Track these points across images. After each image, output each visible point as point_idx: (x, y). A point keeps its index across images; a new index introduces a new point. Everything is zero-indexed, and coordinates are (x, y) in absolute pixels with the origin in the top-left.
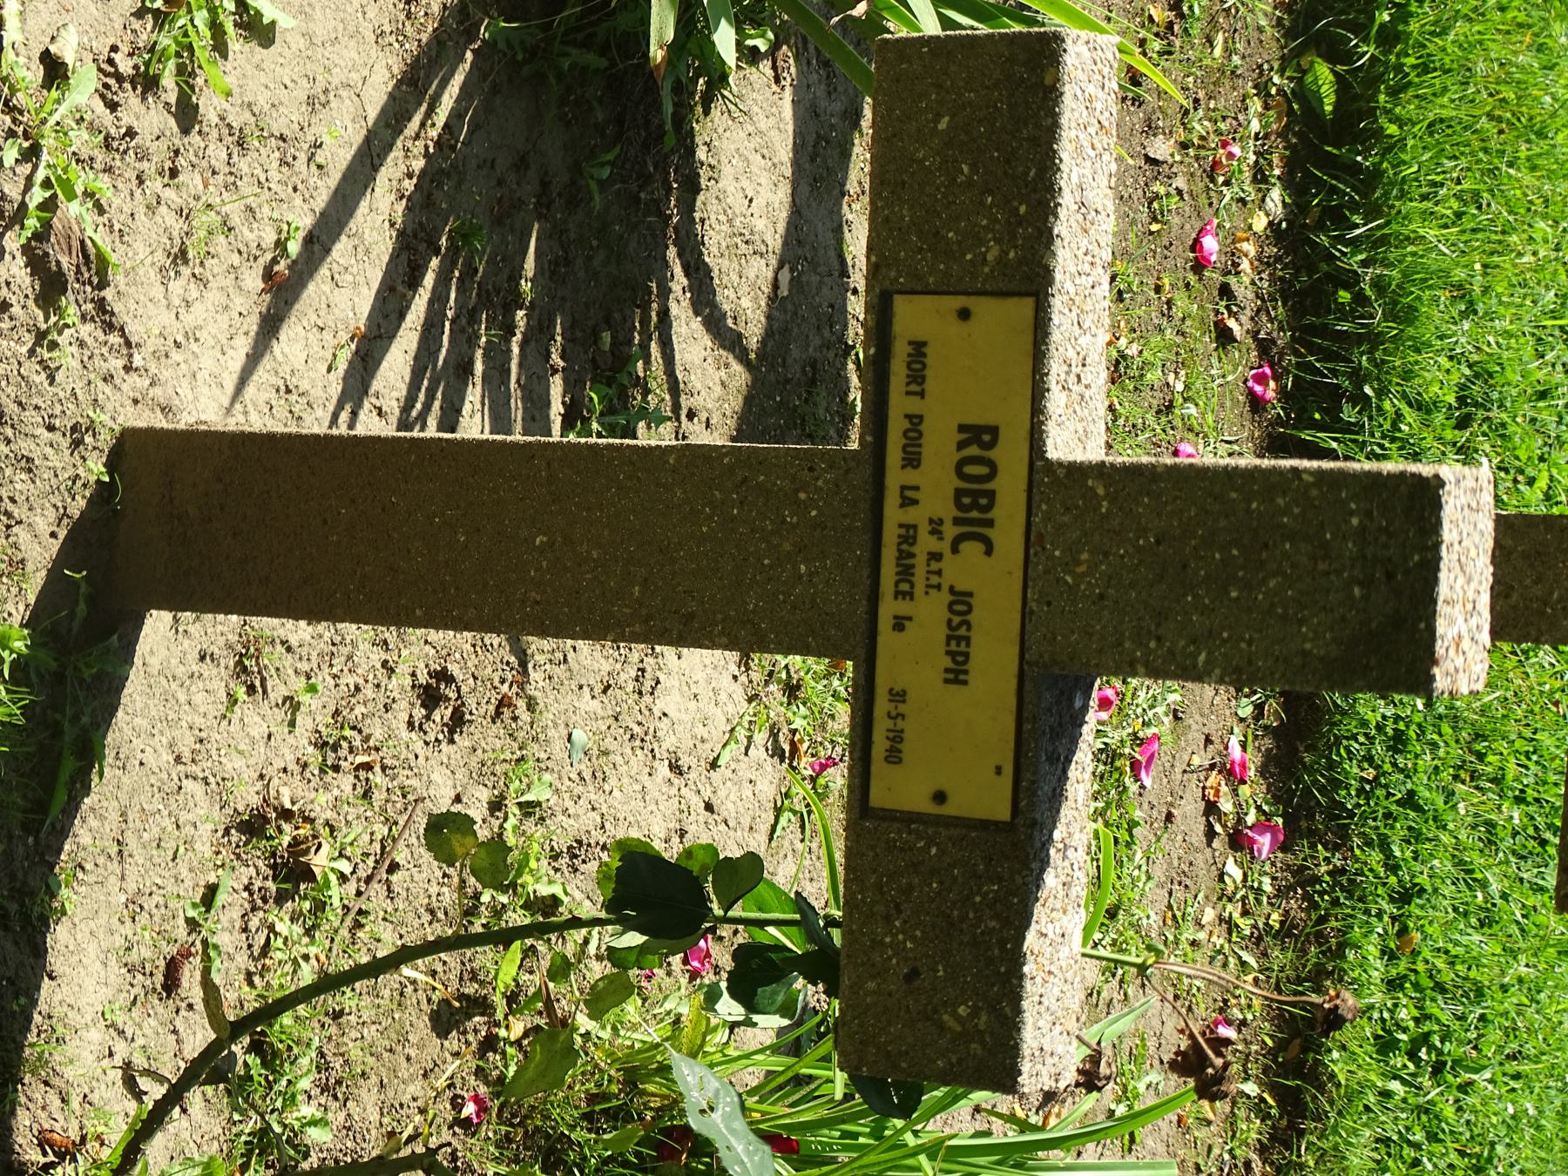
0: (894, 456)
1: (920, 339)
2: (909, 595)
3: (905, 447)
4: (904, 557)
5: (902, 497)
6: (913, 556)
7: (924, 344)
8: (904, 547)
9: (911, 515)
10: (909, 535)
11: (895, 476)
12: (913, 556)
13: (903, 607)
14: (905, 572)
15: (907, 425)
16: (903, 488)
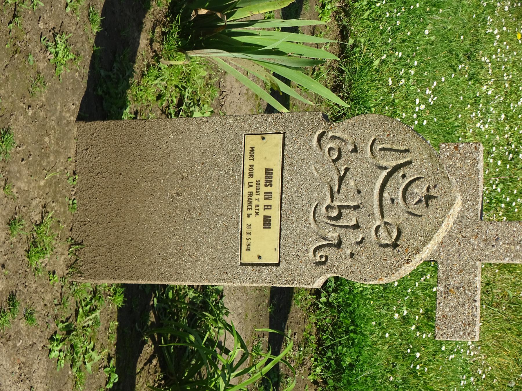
2: (252, 209)
3: (249, 174)
4: (249, 199)
5: (249, 185)
6: (252, 199)
7: (254, 147)
8: (250, 197)
9: (251, 190)
10: (250, 194)
11: (247, 180)
12: (252, 199)
13: (250, 212)
14: (250, 203)
16: (249, 183)
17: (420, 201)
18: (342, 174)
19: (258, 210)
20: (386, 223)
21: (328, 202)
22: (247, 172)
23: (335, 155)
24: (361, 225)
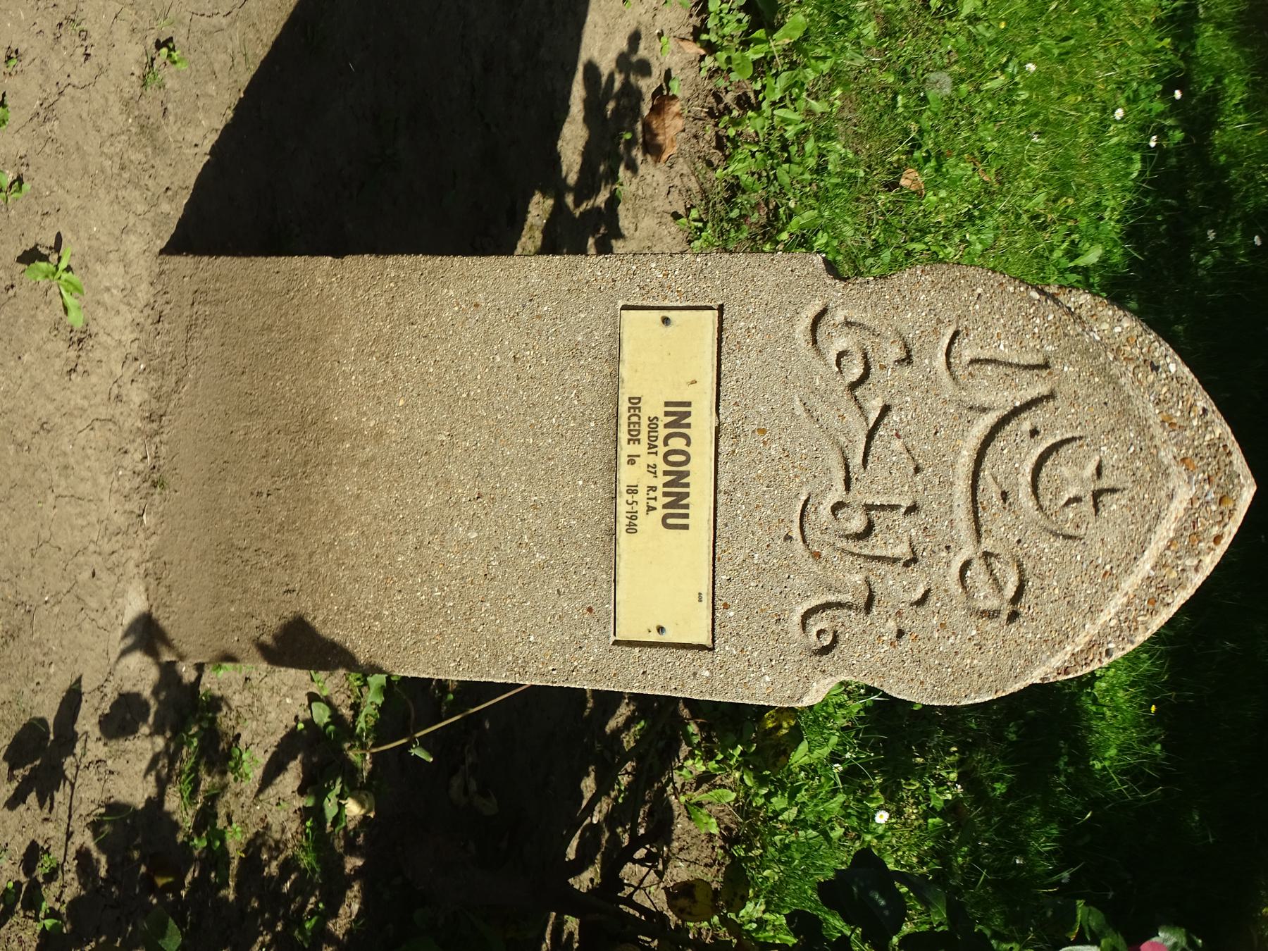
17: (1077, 499)
18: (873, 417)
19: (655, 499)
20: (986, 555)
21: (837, 494)
23: (856, 371)
24: (919, 553)
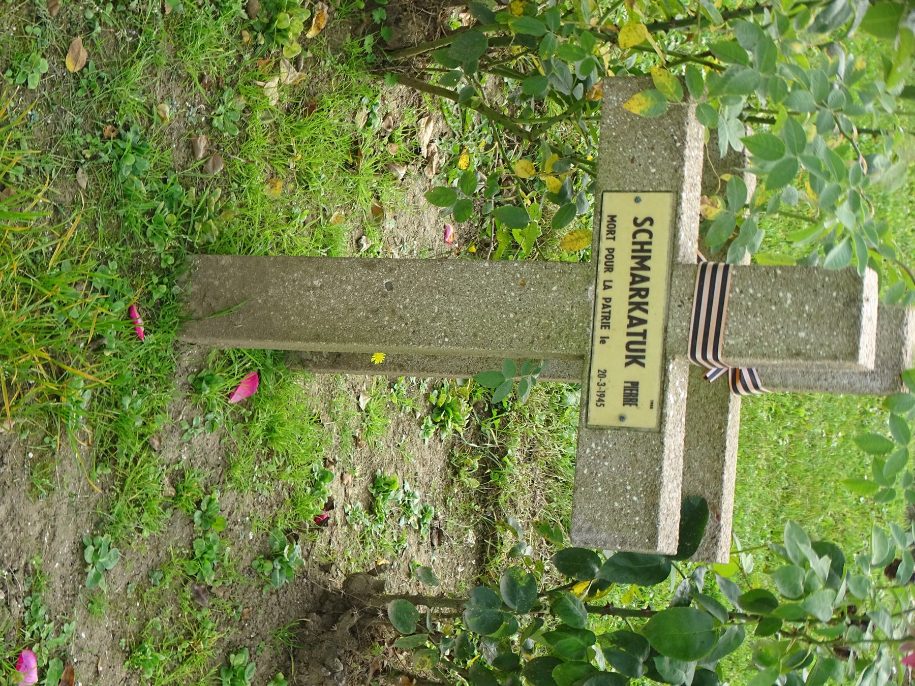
0: (602, 267)
1: (614, 214)
5: (605, 285)
9: (608, 293)
11: (603, 276)
15: (607, 252)
16: (605, 281)
22: (602, 259)
